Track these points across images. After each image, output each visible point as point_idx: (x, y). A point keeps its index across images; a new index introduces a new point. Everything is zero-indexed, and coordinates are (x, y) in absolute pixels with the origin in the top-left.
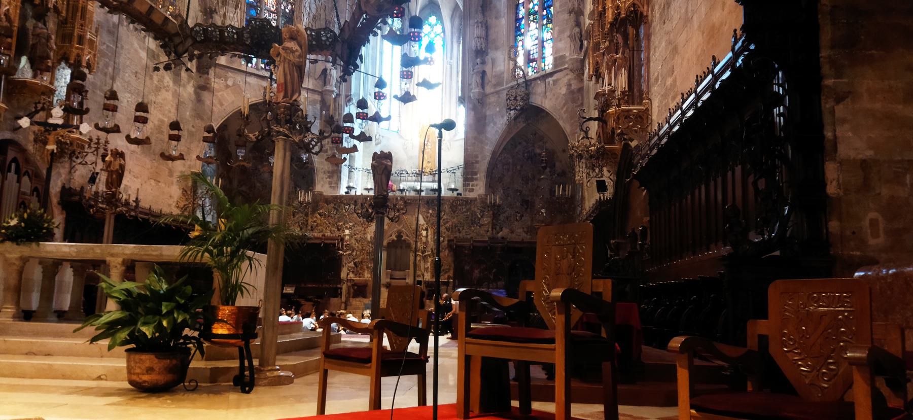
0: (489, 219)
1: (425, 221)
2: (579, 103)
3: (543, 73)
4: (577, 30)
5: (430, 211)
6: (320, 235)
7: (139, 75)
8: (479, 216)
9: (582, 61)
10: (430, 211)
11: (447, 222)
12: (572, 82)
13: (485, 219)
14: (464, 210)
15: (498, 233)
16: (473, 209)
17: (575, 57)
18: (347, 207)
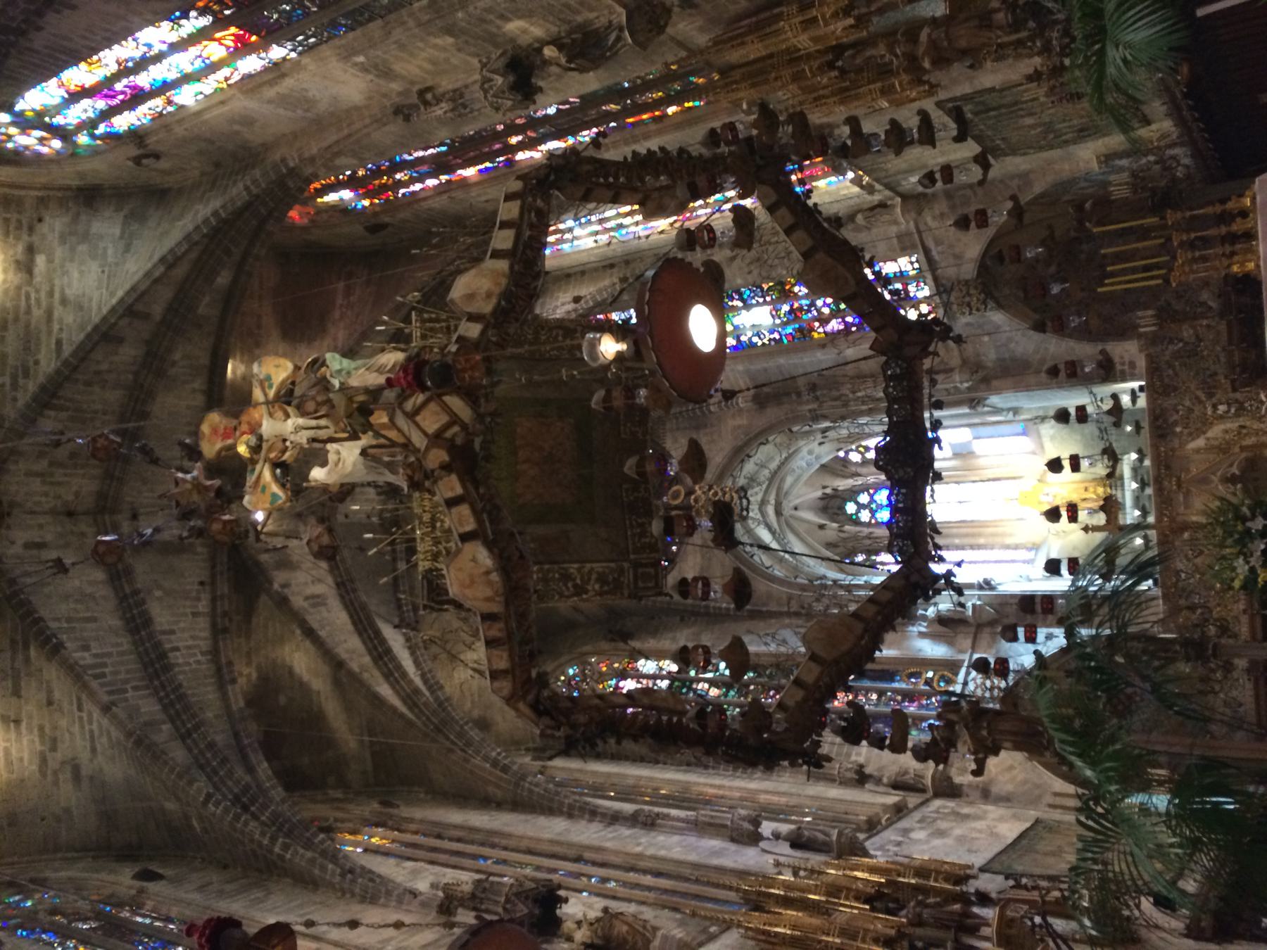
0: (1185, 327)
1: (1198, 437)
2: (969, 192)
3: (925, 267)
4: (860, 218)
5: (1178, 429)
6: (1245, 619)
7: (974, 848)
8: (1181, 345)
9: (905, 197)
10: (1178, 429)
11: (1197, 398)
12: (937, 212)
13: (1185, 334)
14: (1171, 372)
15: (1211, 308)
16: (1167, 358)
17: (898, 210)
18: (1183, 575)
